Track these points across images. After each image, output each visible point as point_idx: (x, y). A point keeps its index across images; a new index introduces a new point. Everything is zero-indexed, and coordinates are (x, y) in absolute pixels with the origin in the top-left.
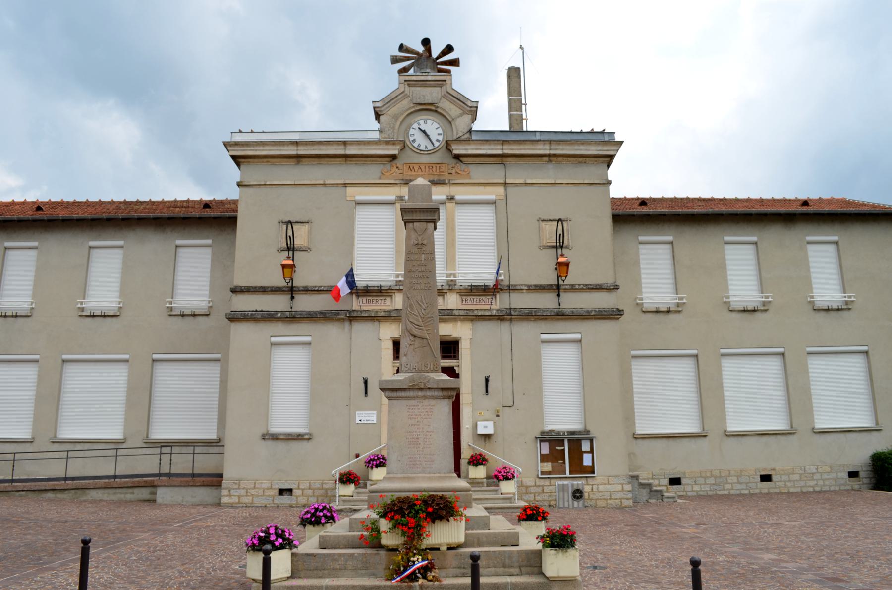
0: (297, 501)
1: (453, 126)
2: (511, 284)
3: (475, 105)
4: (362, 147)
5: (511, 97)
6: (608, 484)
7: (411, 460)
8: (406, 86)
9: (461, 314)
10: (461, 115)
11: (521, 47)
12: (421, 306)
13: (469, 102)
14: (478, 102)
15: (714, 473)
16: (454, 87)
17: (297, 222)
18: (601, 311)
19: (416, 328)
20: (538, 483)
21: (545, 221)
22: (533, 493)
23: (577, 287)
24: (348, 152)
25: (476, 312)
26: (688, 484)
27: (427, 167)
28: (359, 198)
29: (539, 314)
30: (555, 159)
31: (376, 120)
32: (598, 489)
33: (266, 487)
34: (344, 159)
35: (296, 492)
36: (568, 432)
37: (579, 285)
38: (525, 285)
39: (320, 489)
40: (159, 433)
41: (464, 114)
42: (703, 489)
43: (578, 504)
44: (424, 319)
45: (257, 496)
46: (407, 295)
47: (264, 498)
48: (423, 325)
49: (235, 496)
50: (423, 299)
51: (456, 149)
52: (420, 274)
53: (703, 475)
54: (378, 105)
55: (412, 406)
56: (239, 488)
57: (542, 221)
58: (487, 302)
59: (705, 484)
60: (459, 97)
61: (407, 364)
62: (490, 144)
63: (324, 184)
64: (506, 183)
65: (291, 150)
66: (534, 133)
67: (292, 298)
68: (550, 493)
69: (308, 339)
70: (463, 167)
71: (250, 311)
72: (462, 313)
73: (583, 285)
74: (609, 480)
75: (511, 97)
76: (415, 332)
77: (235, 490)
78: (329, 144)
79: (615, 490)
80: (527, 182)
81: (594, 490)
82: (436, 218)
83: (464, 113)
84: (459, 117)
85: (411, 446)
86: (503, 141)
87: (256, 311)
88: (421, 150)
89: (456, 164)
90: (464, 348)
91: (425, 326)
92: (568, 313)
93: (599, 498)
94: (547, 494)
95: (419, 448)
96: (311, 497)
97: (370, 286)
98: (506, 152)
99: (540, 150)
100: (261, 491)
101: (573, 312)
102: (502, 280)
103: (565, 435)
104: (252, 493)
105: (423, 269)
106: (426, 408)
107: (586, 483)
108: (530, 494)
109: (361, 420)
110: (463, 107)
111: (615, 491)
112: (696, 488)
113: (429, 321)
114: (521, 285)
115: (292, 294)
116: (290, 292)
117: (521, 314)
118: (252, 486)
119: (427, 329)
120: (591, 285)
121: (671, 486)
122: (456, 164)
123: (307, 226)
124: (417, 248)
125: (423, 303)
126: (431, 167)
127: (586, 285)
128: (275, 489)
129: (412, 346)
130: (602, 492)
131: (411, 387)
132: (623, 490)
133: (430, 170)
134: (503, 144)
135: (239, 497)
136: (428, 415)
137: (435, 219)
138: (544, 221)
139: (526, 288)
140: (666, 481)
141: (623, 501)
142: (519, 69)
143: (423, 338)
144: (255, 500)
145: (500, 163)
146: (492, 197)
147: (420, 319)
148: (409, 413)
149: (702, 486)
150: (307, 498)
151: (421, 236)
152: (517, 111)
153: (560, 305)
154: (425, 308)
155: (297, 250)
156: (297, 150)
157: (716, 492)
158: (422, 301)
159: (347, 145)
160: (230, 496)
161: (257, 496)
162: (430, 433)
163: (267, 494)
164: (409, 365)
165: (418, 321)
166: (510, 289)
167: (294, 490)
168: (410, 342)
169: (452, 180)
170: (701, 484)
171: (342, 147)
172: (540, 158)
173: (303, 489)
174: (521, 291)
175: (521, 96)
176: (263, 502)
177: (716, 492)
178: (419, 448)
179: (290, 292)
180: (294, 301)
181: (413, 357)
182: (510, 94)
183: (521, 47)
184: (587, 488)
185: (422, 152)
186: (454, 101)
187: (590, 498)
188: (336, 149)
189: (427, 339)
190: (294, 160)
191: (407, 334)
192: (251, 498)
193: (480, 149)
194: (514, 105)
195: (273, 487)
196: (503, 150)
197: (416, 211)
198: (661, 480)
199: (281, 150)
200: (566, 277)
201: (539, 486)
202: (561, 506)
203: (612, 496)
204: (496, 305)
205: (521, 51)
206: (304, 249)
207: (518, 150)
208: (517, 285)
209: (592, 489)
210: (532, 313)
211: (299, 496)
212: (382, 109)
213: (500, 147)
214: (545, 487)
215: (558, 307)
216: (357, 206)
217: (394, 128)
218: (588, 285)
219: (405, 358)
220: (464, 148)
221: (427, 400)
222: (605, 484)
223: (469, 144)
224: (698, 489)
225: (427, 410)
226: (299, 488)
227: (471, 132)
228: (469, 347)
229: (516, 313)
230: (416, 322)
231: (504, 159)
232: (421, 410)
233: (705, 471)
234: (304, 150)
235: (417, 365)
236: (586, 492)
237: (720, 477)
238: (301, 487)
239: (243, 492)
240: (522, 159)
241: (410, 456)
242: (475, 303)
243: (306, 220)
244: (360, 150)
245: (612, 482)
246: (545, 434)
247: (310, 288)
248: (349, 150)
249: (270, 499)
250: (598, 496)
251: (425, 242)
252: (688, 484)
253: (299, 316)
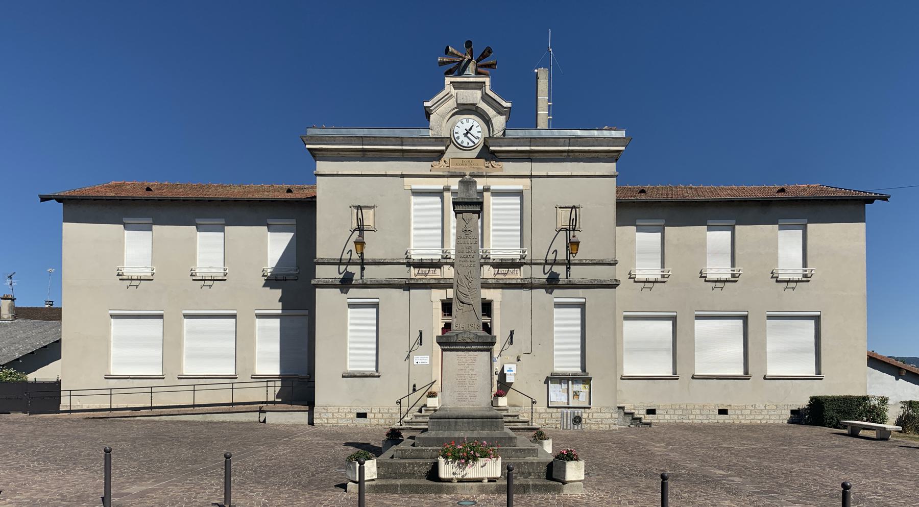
0: (370, 421)
23: (584, 262)
37: (586, 260)
45: (341, 418)
56: (327, 413)
87: (335, 279)
88: (464, 147)
100: (343, 415)
160: (320, 418)
161: (341, 418)
167: (368, 414)
173: (374, 413)
204: (520, 275)
239: (330, 415)
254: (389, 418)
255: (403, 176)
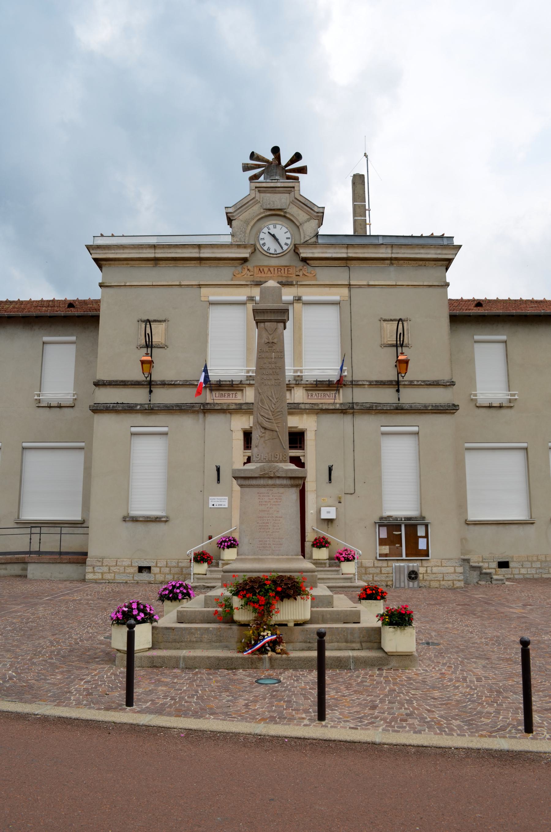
0: (155, 578)
1: (301, 230)
2: (354, 379)
3: (321, 210)
4: (216, 250)
5: (355, 203)
6: (442, 566)
7: (261, 543)
8: (257, 192)
9: (307, 407)
10: (308, 220)
11: (366, 155)
12: (271, 401)
13: (316, 207)
14: (324, 208)
15: (540, 558)
16: (301, 194)
17: (155, 321)
18: (438, 406)
19: (266, 421)
20: (376, 565)
21: (386, 320)
22: (371, 574)
23: (415, 383)
24: (202, 255)
25: (320, 406)
26: (516, 568)
27: (276, 269)
28: (212, 298)
29: (379, 408)
30: (396, 262)
31: (228, 225)
32: (432, 570)
33: (126, 565)
34: (199, 261)
35: (154, 570)
36: (405, 518)
37: (418, 381)
38: (367, 381)
39: (176, 567)
40: (29, 515)
41: (311, 219)
42: (529, 572)
43: (413, 585)
44: (274, 413)
46: (258, 390)
47: (125, 575)
48: (273, 419)
49: (99, 573)
50: (273, 394)
51: (303, 253)
52: (271, 371)
53: (530, 559)
54: (230, 210)
55: (262, 493)
56: (102, 566)
57: (383, 321)
58: (331, 396)
59: (532, 567)
60: (306, 203)
61: (258, 455)
62: (335, 248)
63: (180, 285)
64: (350, 285)
65: (149, 253)
66: (377, 237)
67: (151, 392)
68: (388, 574)
69: (165, 429)
70: (310, 269)
71: (111, 404)
72: (307, 406)
73: (422, 381)
74: (443, 563)
75: (355, 203)
76: (266, 425)
77: (99, 568)
78: (185, 248)
79: (447, 572)
80: (370, 284)
81: (428, 572)
82: (285, 318)
83: (311, 218)
84: (306, 222)
85: (261, 530)
86: (348, 245)
87: (117, 403)
88: (270, 254)
89: (303, 267)
90: (310, 439)
91: (275, 420)
92: (406, 407)
93: (433, 579)
94: (384, 575)
95: (269, 532)
96: (168, 574)
97: (222, 381)
98: (350, 255)
99: (382, 253)
100: (122, 569)
101: (411, 407)
102: (345, 376)
103: (402, 521)
104: (114, 571)
105: (273, 366)
106: (275, 495)
107: (420, 565)
108: (369, 574)
109: (213, 505)
110: (310, 212)
111: (447, 573)
112: (523, 571)
113: (278, 415)
114: (363, 381)
115: (150, 388)
116: (149, 386)
117: (362, 408)
118: (114, 564)
119: (277, 422)
120: (428, 381)
121: (499, 569)
122: (303, 267)
123: (164, 324)
124: (268, 346)
125: (273, 398)
126: (279, 270)
127: (424, 381)
128: (135, 567)
129: (263, 438)
130: (435, 573)
131: (262, 476)
132: (455, 572)
133: (279, 272)
134: (347, 248)
135: (102, 574)
136: (277, 502)
137: (285, 320)
138: (385, 320)
139: (368, 383)
140: (495, 565)
141: (455, 582)
142: (363, 176)
143: (273, 431)
144: (117, 577)
145: (345, 265)
146: (337, 298)
147: (270, 413)
148: (259, 500)
149: (529, 570)
150: (164, 575)
151: (272, 336)
152: (361, 216)
153: (399, 400)
154: (275, 403)
155: (155, 347)
156: (155, 253)
157: (541, 575)
158: (272, 396)
159: (201, 249)
160: (94, 572)
161: (119, 573)
162: (278, 519)
163: (127, 571)
164: (259, 456)
165: (269, 415)
166: (352, 384)
167: (152, 568)
168: (260, 434)
169: (300, 281)
170: (527, 568)
171: (197, 250)
172: (382, 261)
173: (160, 567)
174: (362, 386)
175: (365, 202)
176: (124, 578)
177: (541, 575)
178: (269, 532)
179: (149, 386)
180: (152, 394)
181: (264, 448)
182: (354, 200)
183: (366, 155)
184: (422, 570)
185: (272, 255)
186: (302, 207)
187: (425, 579)
188: (191, 253)
189: (276, 431)
190: (152, 262)
191: (258, 427)
192: (113, 575)
193: (326, 253)
194: (358, 210)
195: (133, 565)
196: (347, 253)
197: (267, 312)
198: (490, 563)
199: (140, 253)
200: (405, 374)
201: (377, 567)
202: (398, 586)
203: (445, 577)
204: (339, 399)
205: (366, 159)
206: (161, 346)
207: (361, 253)
208: (360, 381)
209: (427, 571)
210: (373, 407)
211: (157, 574)
212: (234, 214)
213: (345, 250)
214: (382, 569)
215: (398, 402)
216: (210, 305)
217: (245, 232)
218: (426, 381)
219: (256, 449)
220: (311, 251)
221: (276, 488)
222: (439, 566)
223: (316, 247)
224: (525, 573)
225: (276, 497)
226: (156, 566)
227: (317, 237)
228: (313, 438)
229: (358, 407)
230: (266, 416)
231: (348, 262)
232: (271, 497)
233: (532, 556)
234: (161, 253)
235: (267, 455)
236: (421, 574)
237: (546, 561)
238: (158, 565)
239: (105, 569)
240: (365, 262)
241: (260, 539)
242: (320, 398)
243: (163, 319)
244: (213, 253)
245: (445, 565)
246: (384, 520)
247: (167, 383)
248: (204, 253)
249: (131, 576)
250: (432, 577)
251: (275, 341)
252: (516, 568)
253: (157, 409)
254: (179, 574)
255: (200, 286)
